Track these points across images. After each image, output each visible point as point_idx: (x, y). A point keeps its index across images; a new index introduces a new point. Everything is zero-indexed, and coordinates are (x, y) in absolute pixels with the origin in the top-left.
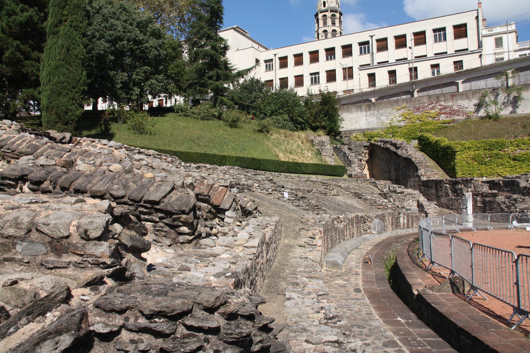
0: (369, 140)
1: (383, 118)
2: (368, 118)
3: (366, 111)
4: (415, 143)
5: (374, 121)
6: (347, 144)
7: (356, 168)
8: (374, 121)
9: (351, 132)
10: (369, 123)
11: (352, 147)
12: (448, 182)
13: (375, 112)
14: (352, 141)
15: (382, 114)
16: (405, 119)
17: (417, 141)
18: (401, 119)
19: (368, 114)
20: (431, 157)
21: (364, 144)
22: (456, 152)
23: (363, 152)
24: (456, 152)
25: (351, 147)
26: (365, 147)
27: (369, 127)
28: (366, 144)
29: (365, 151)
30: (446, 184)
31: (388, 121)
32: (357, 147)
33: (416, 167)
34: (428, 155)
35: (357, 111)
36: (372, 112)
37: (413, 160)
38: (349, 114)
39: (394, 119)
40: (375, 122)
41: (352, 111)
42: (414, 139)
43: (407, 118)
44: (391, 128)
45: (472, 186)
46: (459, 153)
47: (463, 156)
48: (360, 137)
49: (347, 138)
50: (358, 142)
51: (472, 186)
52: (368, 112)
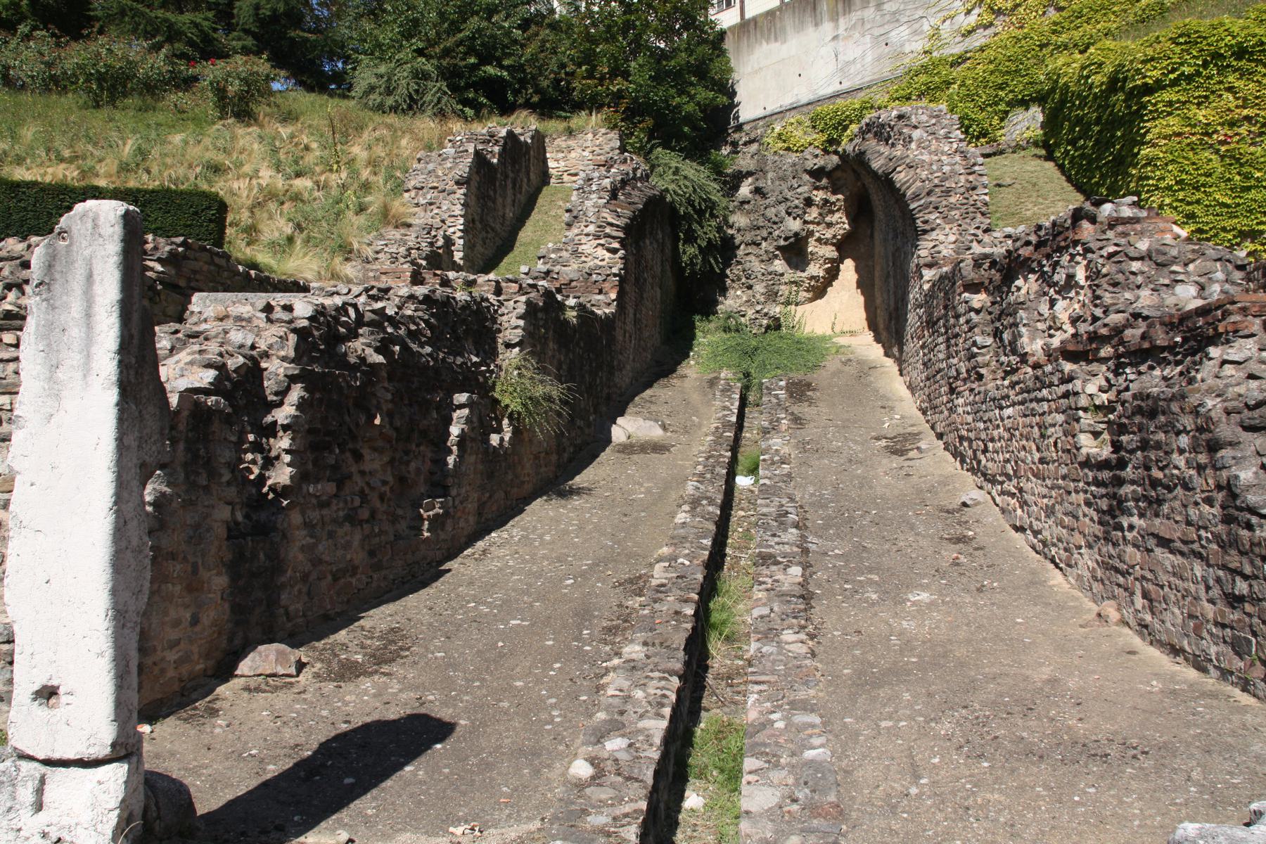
0: (831, 141)
1: (899, 34)
2: (840, 45)
3: (834, 18)
4: (1028, 122)
5: (863, 56)
6: (750, 174)
7: (588, 246)
8: (863, 56)
9: (768, 119)
10: (843, 70)
11: (767, 183)
12: (984, 274)
13: (870, 13)
14: (770, 157)
15: (895, 18)
16: (988, 18)
17: (1036, 115)
18: (972, 19)
19: (841, 31)
20: (1069, 180)
21: (809, 165)
22: (1148, 90)
23: (809, 202)
24: (1148, 90)
25: (761, 184)
26: (817, 174)
27: (846, 85)
28: (820, 162)
29: (819, 196)
30: (974, 287)
31: (919, 45)
32: (783, 179)
33: (910, 217)
34: (1061, 167)
35: (800, 27)
36: (855, 16)
37: (900, 177)
38: (774, 46)
39: (946, 28)
40: (869, 59)
41: (783, 29)
42: (1024, 103)
43: (999, 12)
44: (924, 69)
45: (1081, 275)
46: (1167, 96)
47: (1201, 115)
48: (800, 136)
49: (754, 147)
50: (792, 158)
51: (1081, 275)
52: (842, 21)
